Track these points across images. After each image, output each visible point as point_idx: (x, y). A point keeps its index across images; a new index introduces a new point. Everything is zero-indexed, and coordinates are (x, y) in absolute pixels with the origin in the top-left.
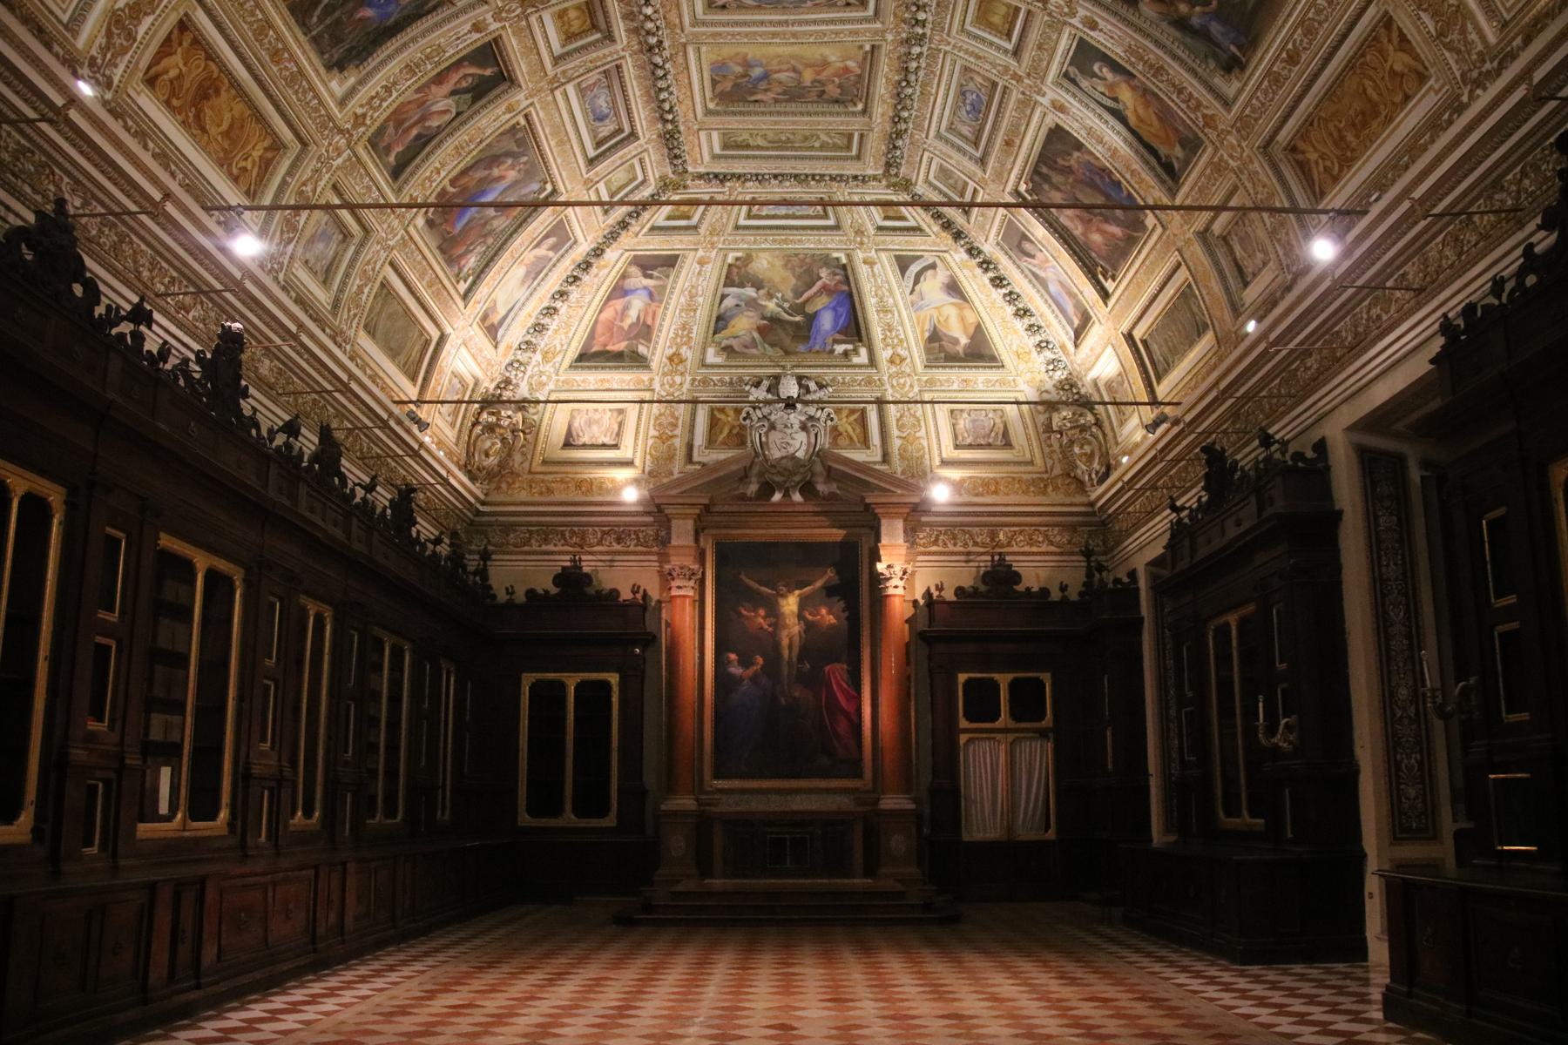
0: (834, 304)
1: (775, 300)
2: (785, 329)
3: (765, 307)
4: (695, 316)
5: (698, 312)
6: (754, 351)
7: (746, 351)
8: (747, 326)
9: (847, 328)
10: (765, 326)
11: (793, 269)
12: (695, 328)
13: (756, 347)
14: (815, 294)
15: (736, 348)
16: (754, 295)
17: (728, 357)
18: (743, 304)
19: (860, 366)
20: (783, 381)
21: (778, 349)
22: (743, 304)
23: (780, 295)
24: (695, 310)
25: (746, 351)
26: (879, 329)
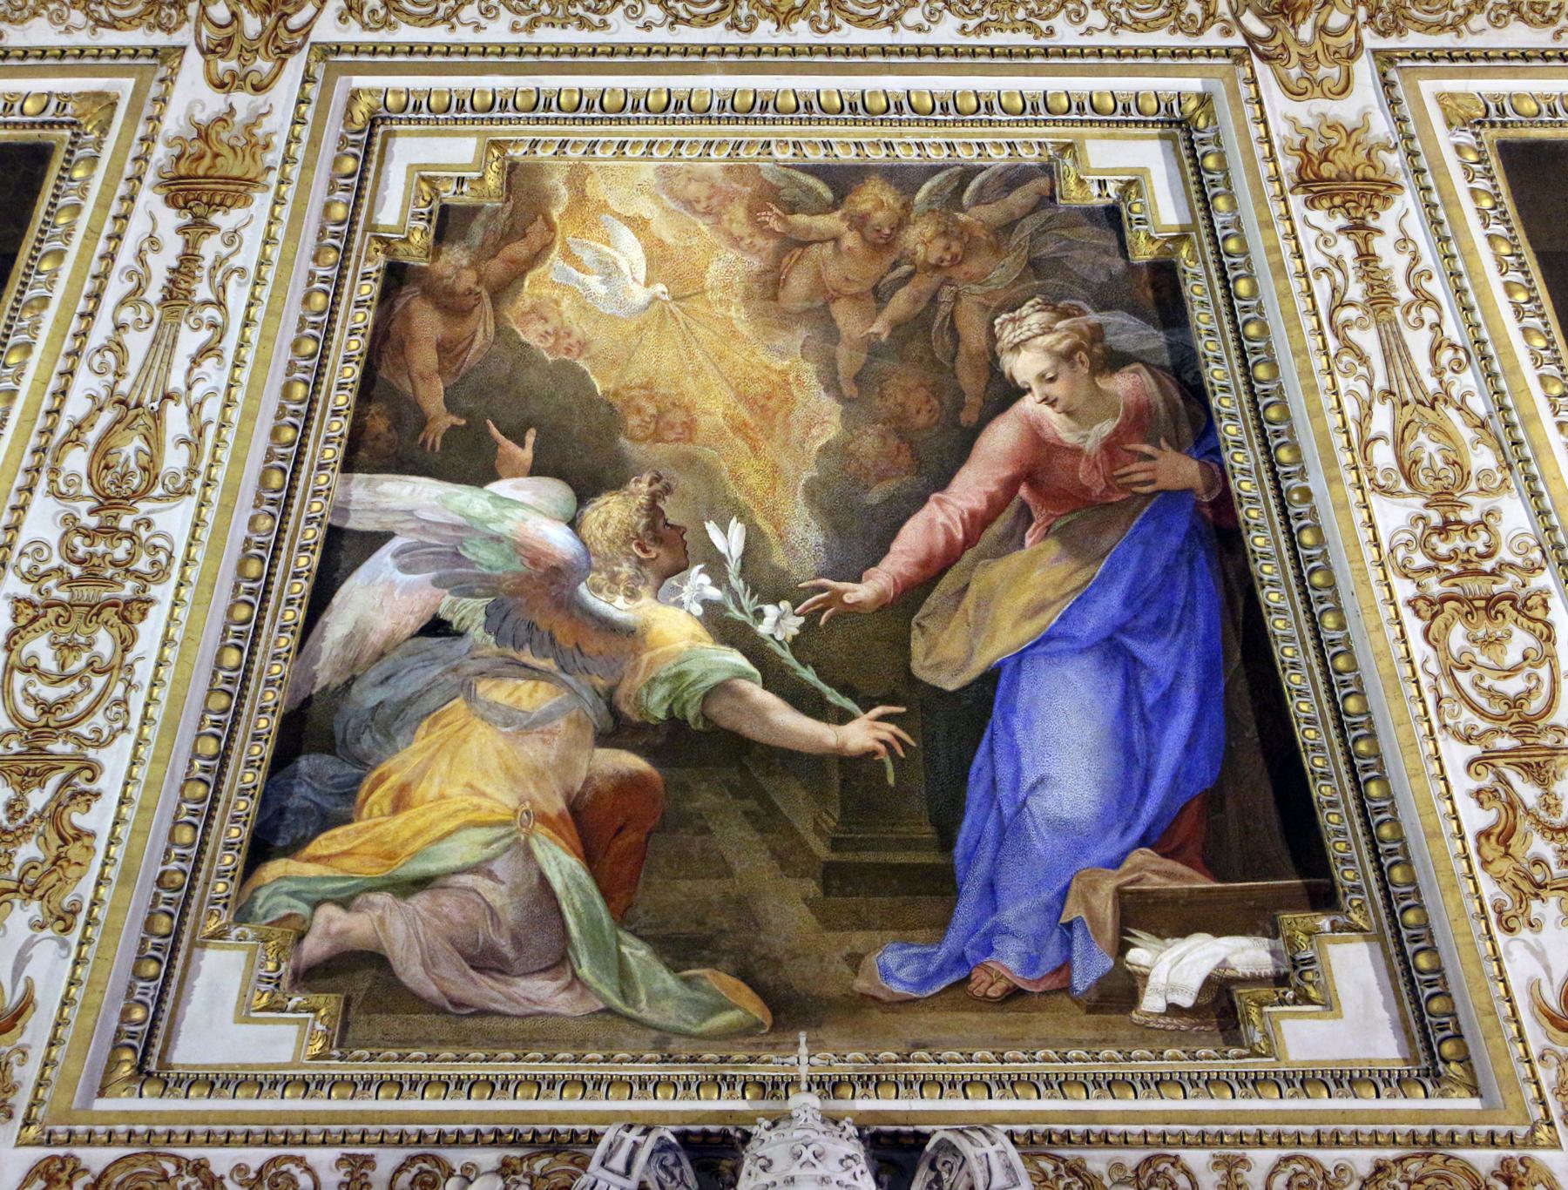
0: (1111, 604)
1: (698, 582)
2: (766, 819)
3: (627, 636)
4: (118, 668)
5: (150, 630)
6: (542, 992)
7: (486, 990)
8: (502, 799)
9: (1213, 799)
10: (629, 785)
11: (820, 315)
12: (114, 760)
13: (559, 962)
14: (977, 524)
15: (412, 972)
16: (558, 540)
17: (342, 1038)
18: (470, 612)
19: (1344, 1079)
20: (769, 1144)
21: (718, 980)
22: (470, 612)
23: (730, 541)
24: (129, 612)
25: (486, 990)
26: (1456, 754)
